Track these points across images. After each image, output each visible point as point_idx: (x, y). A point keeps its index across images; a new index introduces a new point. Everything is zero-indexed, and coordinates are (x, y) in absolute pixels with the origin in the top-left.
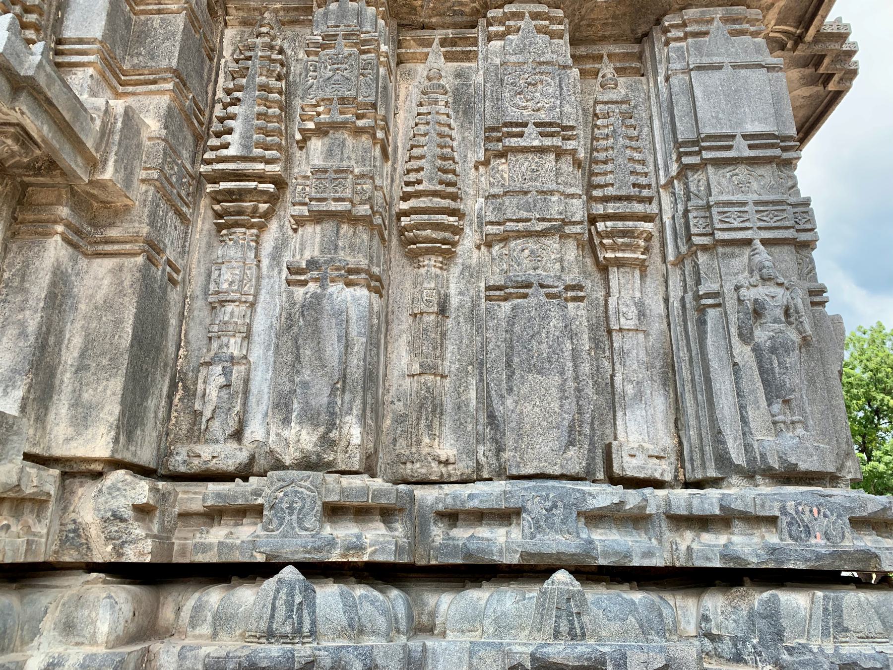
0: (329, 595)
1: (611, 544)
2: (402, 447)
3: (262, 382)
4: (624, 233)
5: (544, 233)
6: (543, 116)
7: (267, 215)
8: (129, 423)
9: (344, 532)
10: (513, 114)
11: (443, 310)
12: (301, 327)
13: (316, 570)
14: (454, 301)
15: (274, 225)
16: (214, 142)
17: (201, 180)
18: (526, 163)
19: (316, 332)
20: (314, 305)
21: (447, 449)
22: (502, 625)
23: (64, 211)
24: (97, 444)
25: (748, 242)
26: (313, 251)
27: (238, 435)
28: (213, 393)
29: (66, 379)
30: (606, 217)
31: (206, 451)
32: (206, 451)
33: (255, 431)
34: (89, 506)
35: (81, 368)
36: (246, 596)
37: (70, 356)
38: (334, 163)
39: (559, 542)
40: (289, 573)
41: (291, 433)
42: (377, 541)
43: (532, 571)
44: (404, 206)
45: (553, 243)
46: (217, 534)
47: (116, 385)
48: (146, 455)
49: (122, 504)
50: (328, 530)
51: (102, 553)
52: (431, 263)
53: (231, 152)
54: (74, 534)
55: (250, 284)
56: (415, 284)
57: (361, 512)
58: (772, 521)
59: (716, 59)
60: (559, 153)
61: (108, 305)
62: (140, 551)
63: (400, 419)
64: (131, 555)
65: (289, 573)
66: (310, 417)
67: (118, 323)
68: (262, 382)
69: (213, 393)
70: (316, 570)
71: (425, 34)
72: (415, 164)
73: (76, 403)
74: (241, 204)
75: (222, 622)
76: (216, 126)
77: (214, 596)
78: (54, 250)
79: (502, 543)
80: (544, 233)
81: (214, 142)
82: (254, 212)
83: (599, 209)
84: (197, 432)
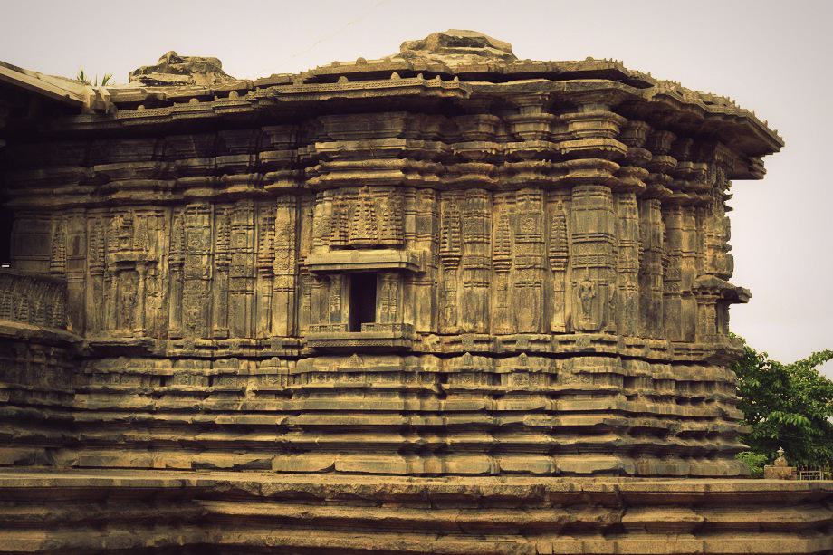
0: (475, 358)
1: (535, 347)
2: (496, 326)
3: (460, 311)
4: (558, 262)
5: (530, 268)
6: (530, 232)
7: (457, 266)
8: (432, 325)
9: (478, 346)
10: (523, 231)
11: (506, 289)
12: (468, 298)
13: (473, 354)
14: (509, 286)
15: (459, 268)
16: (442, 245)
17: (440, 257)
18: (526, 247)
19: (470, 299)
20: (470, 294)
21: (507, 327)
22: (511, 364)
23: (414, 279)
24: (427, 329)
25: (585, 268)
26: (469, 279)
27: (455, 325)
28: (449, 314)
29: (418, 315)
30: (554, 258)
31: (449, 329)
32: (449, 329)
33: (459, 324)
34: (429, 341)
35: (421, 312)
36: (460, 359)
37: (418, 310)
38: (473, 254)
39: (524, 347)
40: (467, 354)
41: (467, 324)
42: (485, 347)
43: (516, 354)
44: (494, 259)
45: (532, 271)
46: (453, 347)
47: (429, 316)
48: (436, 331)
49: (434, 341)
50: (475, 345)
51: (432, 351)
52: (503, 275)
53: (446, 250)
54: (426, 347)
55: (458, 286)
56: (499, 281)
57: (482, 342)
58: (574, 342)
59: (584, 207)
60: (535, 243)
61: (425, 298)
62: (439, 350)
63: (495, 319)
64: (437, 351)
65: (467, 354)
66: (471, 321)
67: (428, 302)
68: (460, 311)
69: (449, 314)
70: (473, 354)
71: (501, 195)
72: (498, 244)
73: (421, 320)
74: (449, 263)
75: (456, 363)
76: (442, 241)
77: (454, 359)
78: (414, 288)
79: (512, 348)
80: (530, 268)
81: (442, 245)
82: (454, 265)
83: (550, 254)
84: (446, 323)
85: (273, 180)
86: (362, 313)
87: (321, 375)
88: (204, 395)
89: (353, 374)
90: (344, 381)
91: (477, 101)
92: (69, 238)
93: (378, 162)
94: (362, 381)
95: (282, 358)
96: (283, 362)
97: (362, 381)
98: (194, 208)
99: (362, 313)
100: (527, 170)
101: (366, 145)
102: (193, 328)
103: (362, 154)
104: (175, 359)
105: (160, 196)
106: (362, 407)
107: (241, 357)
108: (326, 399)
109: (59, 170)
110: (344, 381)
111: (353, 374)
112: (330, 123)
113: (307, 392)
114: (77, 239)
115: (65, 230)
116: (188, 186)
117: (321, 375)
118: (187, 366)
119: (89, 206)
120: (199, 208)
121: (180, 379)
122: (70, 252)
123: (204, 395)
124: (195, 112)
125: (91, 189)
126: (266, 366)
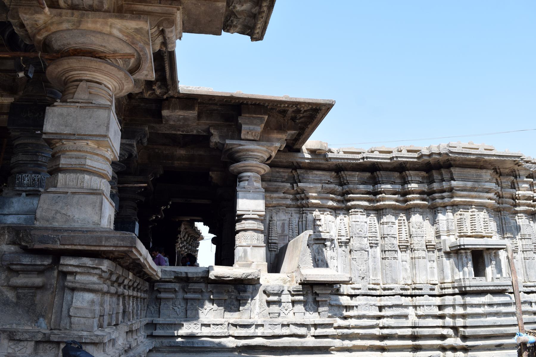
85: (413, 199)
86: (479, 271)
87: (472, 306)
88: (379, 318)
89: (491, 305)
90: (487, 309)
91: (507, 170)
92: (279, 223)
93: (481, 194)
94: (495, 309)
95: (430, 295)
96: (431, 298)
97: (495, 309)
98: (358, 212)
99: (479, 271)
100: (524, 205)
101: (476, 185)
102: (363, 278)
103: (472, 190)
104: (352, 296)
105: (335, 204)
106: (499, 324)
107: (402, 295)
108: (482, 319)
109: (276, 183)
110: (487, 309)
111: (491, 305)
112: (456, 171)
113: (463, 316)
114: (283, 224)
115: (275, 218)
116: (353, 199)
117: (472, 306)
118: (367, 300)
119: (288, 206)
120: (360, 212)
121: (363, 308)
122: (279, 231)
123: (379, 318)
124: (378, 158)
125: (291, 196)
126: (418, 301)
